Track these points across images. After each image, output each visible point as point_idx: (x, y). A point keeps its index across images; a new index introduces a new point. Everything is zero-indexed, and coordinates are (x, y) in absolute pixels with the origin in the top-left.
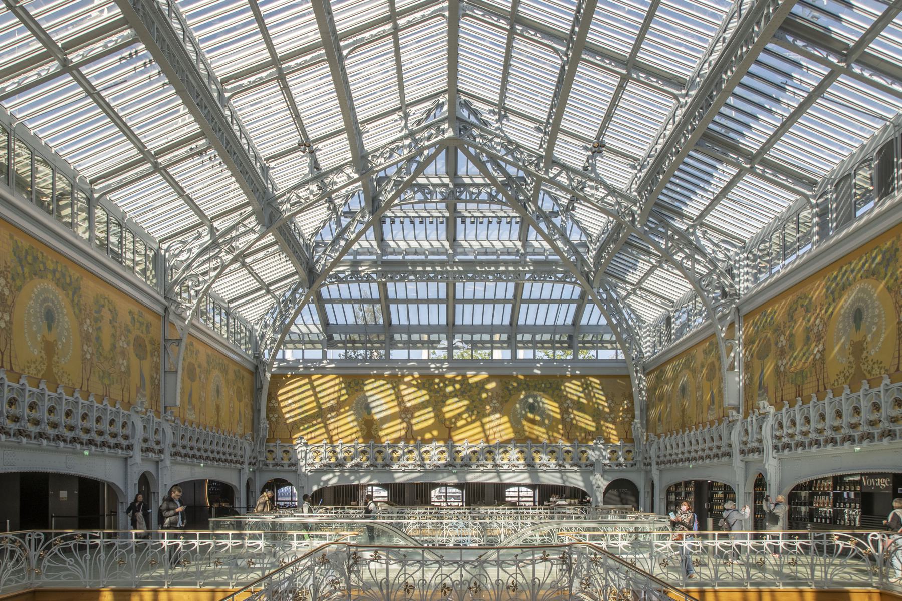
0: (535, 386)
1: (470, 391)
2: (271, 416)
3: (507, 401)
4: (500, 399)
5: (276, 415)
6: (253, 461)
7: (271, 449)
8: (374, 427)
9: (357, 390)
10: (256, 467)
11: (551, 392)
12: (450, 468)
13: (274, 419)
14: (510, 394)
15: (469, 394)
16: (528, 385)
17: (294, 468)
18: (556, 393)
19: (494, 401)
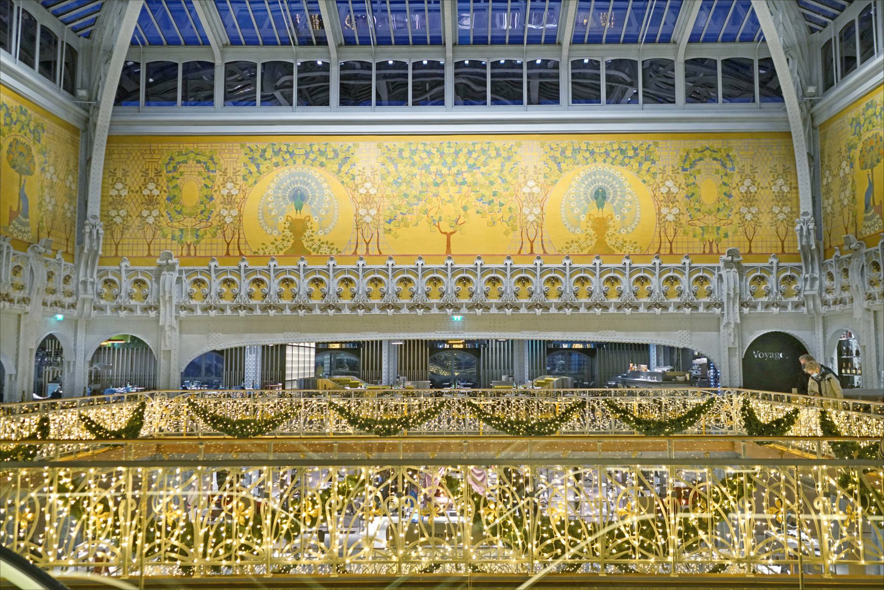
0: (607, 154)
1: (485, 164)
2: (113, 213)
3: (554, 183)
4: (541, 179)
5: (123, 213)
6: (69, 300)
7: (110, 277)
8: (308, 233)
9: (277, 165)
10: (75, 313)
11: (636, 166)
12: (449, 311)
13: (118, 220)
14: (560, 170)
15: (483, 169)
16: (592, 153)
17: (152, 314)
18: (645, 166)
19: (531, 183)
